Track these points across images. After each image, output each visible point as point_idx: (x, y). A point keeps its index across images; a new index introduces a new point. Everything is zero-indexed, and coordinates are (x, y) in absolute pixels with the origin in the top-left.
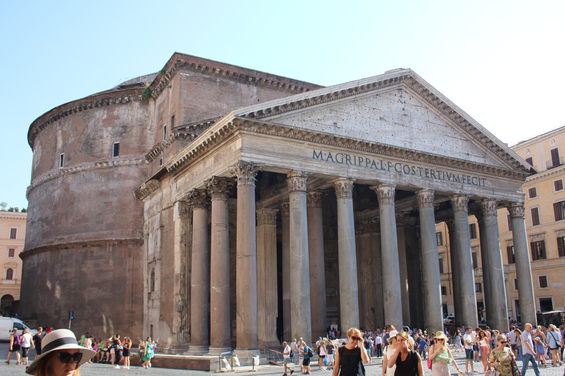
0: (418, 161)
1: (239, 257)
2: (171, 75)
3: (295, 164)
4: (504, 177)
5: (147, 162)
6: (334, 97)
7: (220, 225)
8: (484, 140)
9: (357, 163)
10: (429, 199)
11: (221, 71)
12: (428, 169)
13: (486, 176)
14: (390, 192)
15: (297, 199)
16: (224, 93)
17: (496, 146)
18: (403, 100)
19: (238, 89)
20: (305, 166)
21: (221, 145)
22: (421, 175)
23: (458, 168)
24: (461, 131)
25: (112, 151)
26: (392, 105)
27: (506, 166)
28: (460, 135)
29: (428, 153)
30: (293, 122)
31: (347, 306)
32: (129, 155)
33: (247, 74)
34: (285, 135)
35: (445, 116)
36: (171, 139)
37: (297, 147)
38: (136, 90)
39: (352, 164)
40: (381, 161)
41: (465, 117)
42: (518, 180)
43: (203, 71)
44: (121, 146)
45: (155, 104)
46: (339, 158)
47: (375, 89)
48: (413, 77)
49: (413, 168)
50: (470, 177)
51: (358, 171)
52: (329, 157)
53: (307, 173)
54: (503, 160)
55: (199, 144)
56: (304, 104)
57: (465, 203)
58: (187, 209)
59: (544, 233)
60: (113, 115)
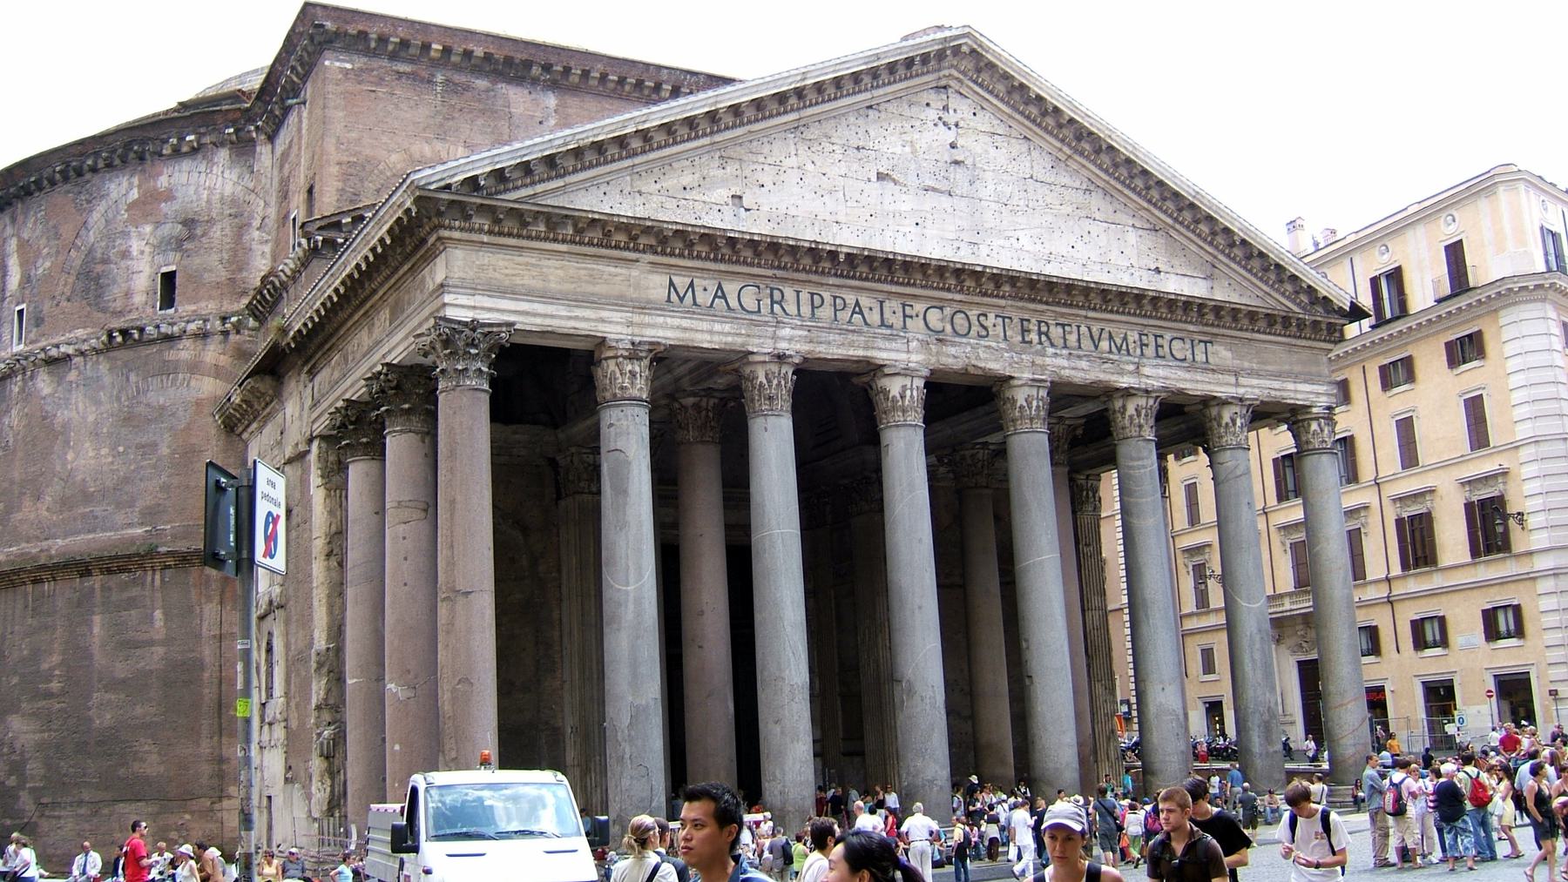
0: (997, 296)
1: (444, 596)
2: (303, 68)
3: (610, 322)
4: (1270, 333)
5: (252, 322)
6: (729, 120)
7: (407, 504)
9: (806, 310)
10: (1030, 408)
11: (447, 51)
12: (1028, 320)
14: (908, 393)
15: (618, 423)
16: (457, 115)
17: (1244, 242)
18: (951, 118)
19: (500, 102)
20: (642, 325)
21: (401, 272)
23: (1123, 313)
25: (156, 293)
26: (916, 136)
27: (1278, 302)
28: (1132, 213)
29: (1023, 275)
30: (606, 197)
31: (778, 729)
32: (203, 304)
33: (525, 57)
34: (578, 239)
35: (1084, 162)
36: (301, 254)
37: (618, 270)
38: (217, 117)
39: (787, 314)
40: (881, 303)
41: (1142, 160)
42: (1315, 339)
43: (391, 52)
44: (178, 280)
45: (272, 153)
46: (749, 301)
47: (860, 92)
48: (979, 50)
49: (982, 318)
51: (806, 333)
52: (716, 296)
53: (647, 347)
54: (1266, 283)
55: (348, 270)
56: (636, 144)
57: (1146, 415)
59: (1432, 491)
60: (156, 189)
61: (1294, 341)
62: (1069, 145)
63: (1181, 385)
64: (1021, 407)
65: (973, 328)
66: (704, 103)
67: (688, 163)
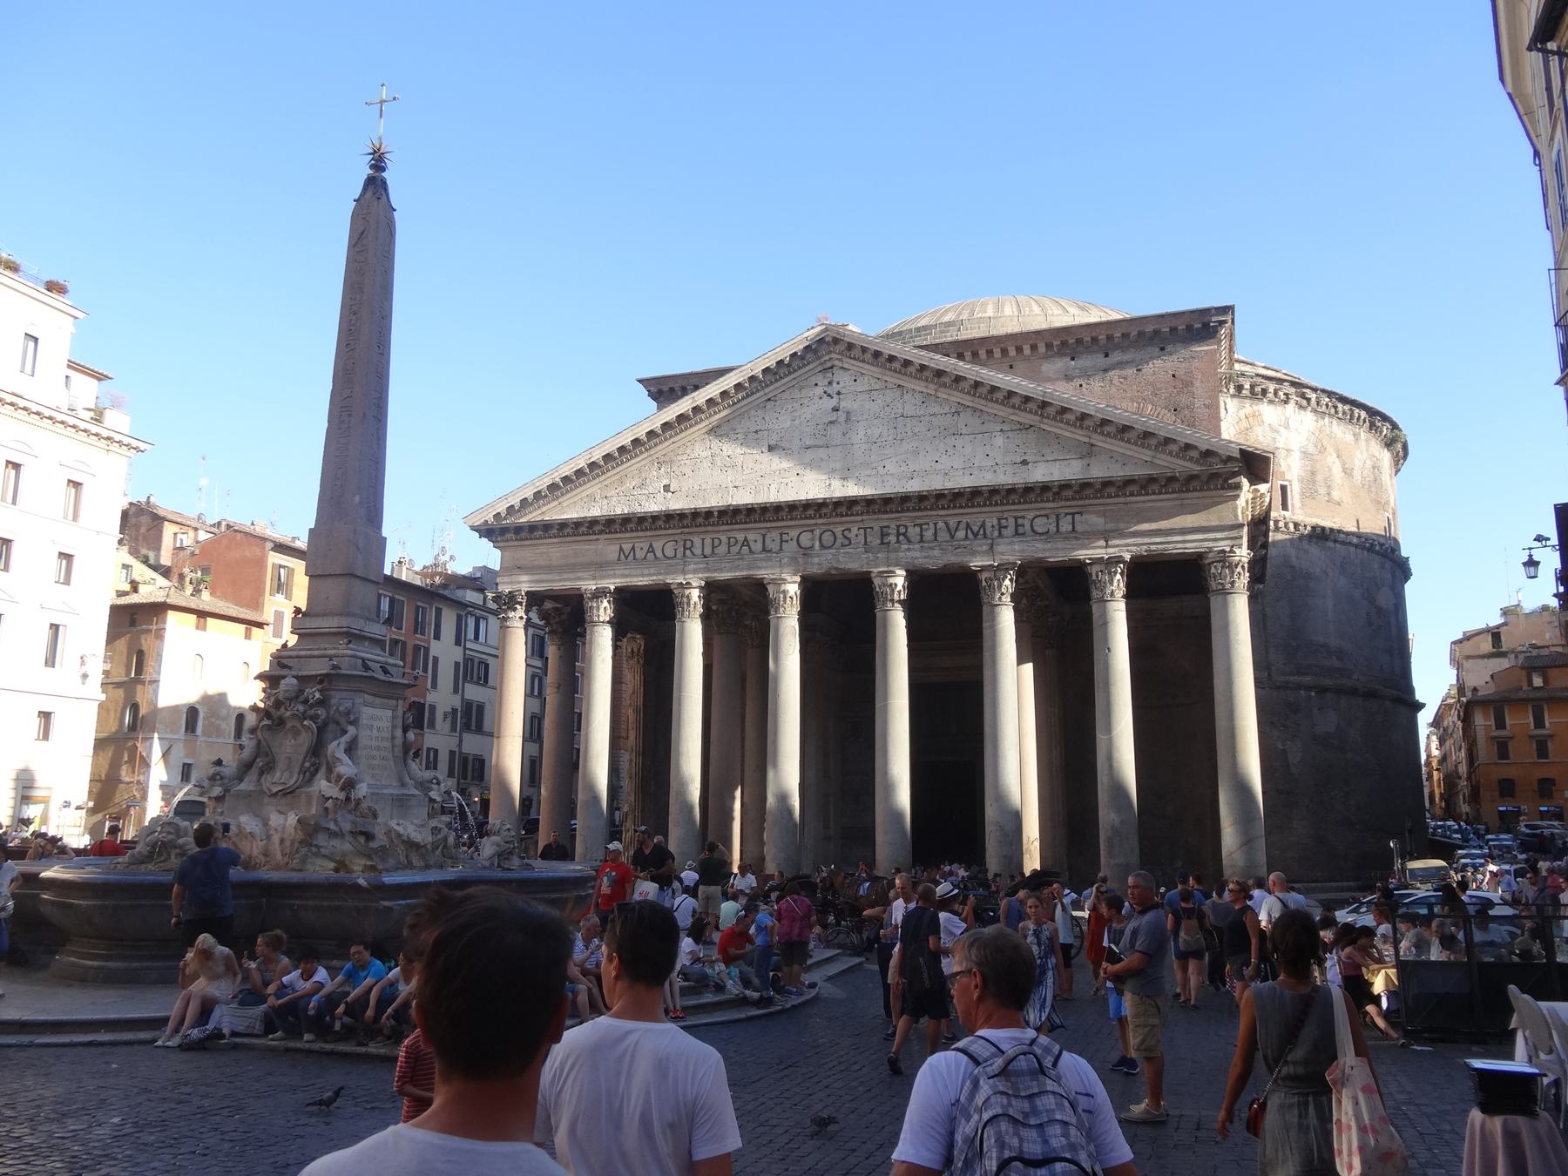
0: (852, 515)
4: (1147, 494)
8: (1069, 416)
9: (708, 550)
12: (888, 527)
23: (973, 506)
24: (1003, 411)
40: (764, 536)
42: (1209, 490)
46: (669, 553)
49: (846, 532)
50: (1023, 517)
51: (705, 565)
52: (648, 552)
54: (1149, 447)
58: (636, 650)
62: (932, 382)
63: (1040, 555)
64: (878, 592)
66: (624, 437)
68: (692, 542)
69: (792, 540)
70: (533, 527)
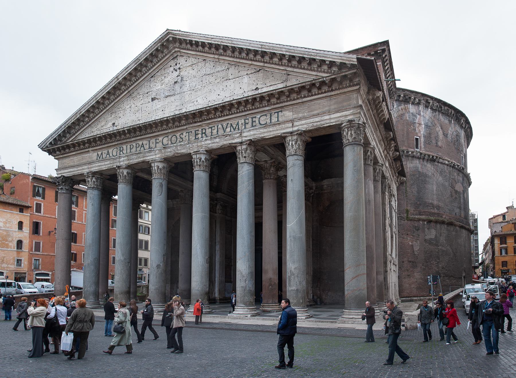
0: (182, 126)
3: (85, 169)
4: (312, 95)
9: (129, 151)
13: (281, 107)
18: (178, 66)
20: (91, 168)
22: (189, 140)
23: (232, 114)
42: (343, 88)
47: (144, 74)
51: (127, 158)
52: (107, 154)
53: (90, 173)
54: (314, 70)
61: (329, 94)
62: (216, 54)
63: (262, 136)
65: (178, 140)
67: (103, 119)
68: (123, 148)
69: (160, 142)
70: (64, 148)
